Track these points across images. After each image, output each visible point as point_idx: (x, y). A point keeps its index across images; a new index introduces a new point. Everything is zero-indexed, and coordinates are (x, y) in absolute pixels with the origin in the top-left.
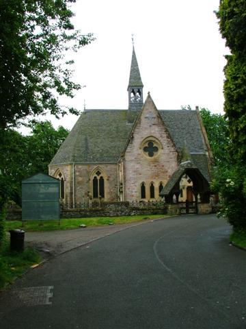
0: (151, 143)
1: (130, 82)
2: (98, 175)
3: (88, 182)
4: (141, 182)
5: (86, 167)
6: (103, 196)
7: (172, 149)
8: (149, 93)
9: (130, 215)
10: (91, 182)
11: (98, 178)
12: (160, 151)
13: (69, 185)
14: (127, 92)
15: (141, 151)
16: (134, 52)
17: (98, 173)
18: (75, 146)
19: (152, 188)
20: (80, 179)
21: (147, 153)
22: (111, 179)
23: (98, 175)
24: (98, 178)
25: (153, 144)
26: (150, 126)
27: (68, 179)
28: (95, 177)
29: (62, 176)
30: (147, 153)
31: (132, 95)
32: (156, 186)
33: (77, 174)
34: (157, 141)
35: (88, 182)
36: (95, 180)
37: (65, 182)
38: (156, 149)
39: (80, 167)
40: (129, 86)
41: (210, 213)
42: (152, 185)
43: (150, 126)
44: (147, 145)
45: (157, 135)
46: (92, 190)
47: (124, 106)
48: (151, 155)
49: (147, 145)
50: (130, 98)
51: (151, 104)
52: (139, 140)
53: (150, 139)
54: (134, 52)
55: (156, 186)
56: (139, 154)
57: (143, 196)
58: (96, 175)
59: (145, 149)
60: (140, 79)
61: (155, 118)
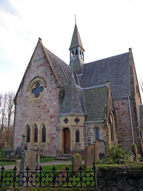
4: (26, 124)
7: (54, 85)
8: (40, 39)
16: (76, 26)
19: (36, 130)
21: (34, 94)
26: (38, 67)
30: (34, 94)
32: (39, 128)
49: (34, 87)
51: (41, 47)
53: (37, 79)
54: (76, 26)
55: (39, 128)
59: (33, 91)
61: (42, 59)
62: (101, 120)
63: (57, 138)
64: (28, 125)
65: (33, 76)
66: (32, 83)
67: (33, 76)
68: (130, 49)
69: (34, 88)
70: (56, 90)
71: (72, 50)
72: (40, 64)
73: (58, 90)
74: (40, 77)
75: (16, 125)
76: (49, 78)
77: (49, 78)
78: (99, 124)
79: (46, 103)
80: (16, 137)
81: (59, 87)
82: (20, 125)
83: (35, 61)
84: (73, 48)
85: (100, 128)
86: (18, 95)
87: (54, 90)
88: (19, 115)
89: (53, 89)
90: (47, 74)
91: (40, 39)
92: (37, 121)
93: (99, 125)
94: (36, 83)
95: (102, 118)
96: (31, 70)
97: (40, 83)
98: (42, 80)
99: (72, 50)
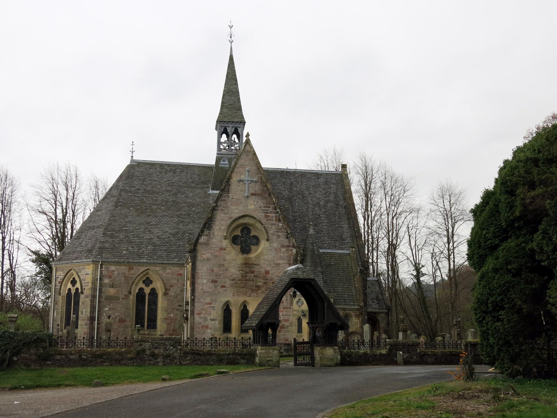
0: (246, 229)
1: (220, 114)
2: (147, 285)
3: (126, 297)
4: (224, 300)
5: (124, 269)
6: (152, 324)
9: (181, 364)
10: (132, 297)
11: (147, 290)
12: (264, 244)
13: (88, 301)
14: (215, 133)
15: (226, 243)
16: (231, 58)
17: (148, 282)
18: (106, 229)
20: (112, 291)
22: (172, 293)
23: (147, 285)
24: (147, 290)
25: (249, 231)
27: (87, 291)
28: (141, 289)
29: (78, 285)
30: (238, 248)
31: (224, 136)
33: (106, 281)
34: (258, 225)
35: (126, 297)
36: (140, 295)
37: (82, 296)
38: (257, 241)
39: (113, 268)
40: (218, 122)
41: (337, 365)
42: (245, 307)
43: (248, 197)
44: (238, 233)
45: (260, 215)
46: (133, 314)
47: (210, 159)
48: (245, 250)
49: (238, 233)
50: (219, 143)
51: (251, 156)
52: (224, 223)
54: (231, 58)
56: (222, 249)
57: (227, 328)
58: (143, 286)
59: (235, 240)
60: (240, 109)
61: (256, 182)
62: (354, 305)
63: (290, 327)
64: (228, 301)
65: (237, 211)
66: (234, 226)
67: (237, 211)
68: (344, 166)
69: (236, 234)
70: (287, 250)
71: (225, 125)
72: (254, 192)
73: (292, 250)
74: (255, 218)
75: (196, 300)
76: (272, 224)
77: (272, 224)
78: (352, 310)
79: (268, 268)
80: (199, 323)
81: (294, 246)
82: (208, 300)
83: (240, 181)
84: (229, 122)
85: (352, 316)
86: (200, 241)
87: (283, 250)
88: (205, 281)
89: (283, 246)
90: (269, 216)
91: (248, 133)
92: (250, 296)
93: (351, 312)
94: (243, 227)
95: (355, 304)
96: (231, 197)
97: (251, 228)
98: (258, 225)
99: (225, 125)
